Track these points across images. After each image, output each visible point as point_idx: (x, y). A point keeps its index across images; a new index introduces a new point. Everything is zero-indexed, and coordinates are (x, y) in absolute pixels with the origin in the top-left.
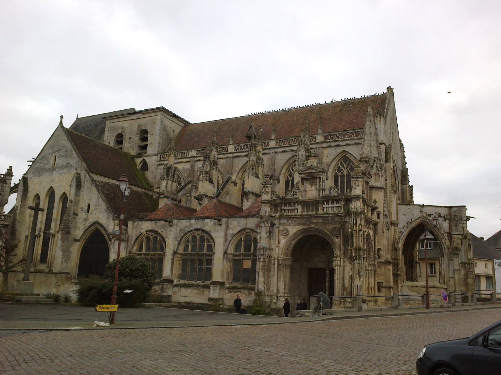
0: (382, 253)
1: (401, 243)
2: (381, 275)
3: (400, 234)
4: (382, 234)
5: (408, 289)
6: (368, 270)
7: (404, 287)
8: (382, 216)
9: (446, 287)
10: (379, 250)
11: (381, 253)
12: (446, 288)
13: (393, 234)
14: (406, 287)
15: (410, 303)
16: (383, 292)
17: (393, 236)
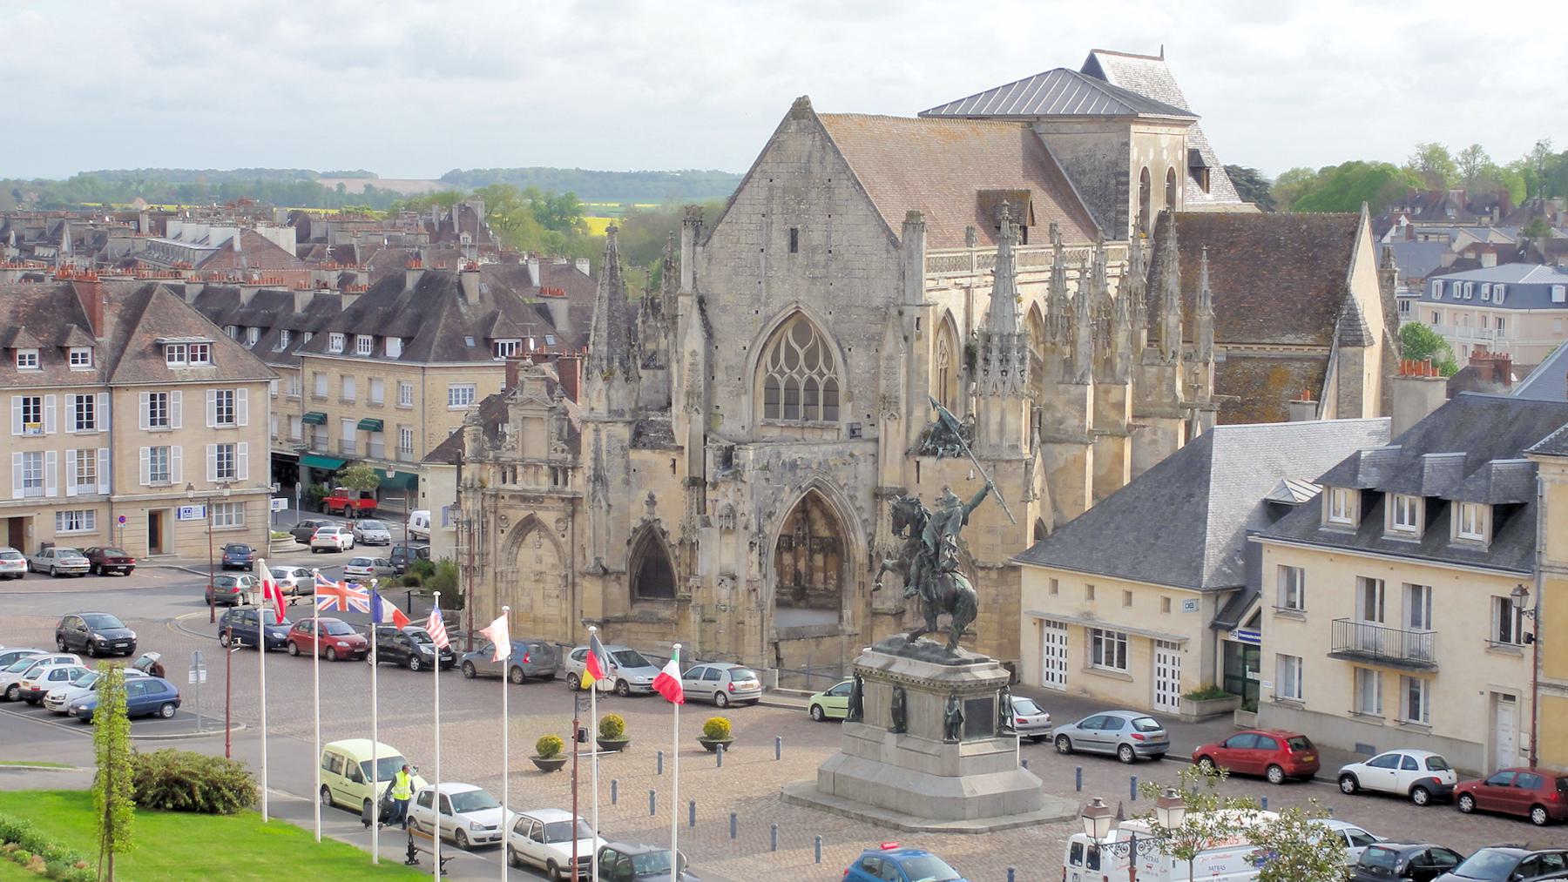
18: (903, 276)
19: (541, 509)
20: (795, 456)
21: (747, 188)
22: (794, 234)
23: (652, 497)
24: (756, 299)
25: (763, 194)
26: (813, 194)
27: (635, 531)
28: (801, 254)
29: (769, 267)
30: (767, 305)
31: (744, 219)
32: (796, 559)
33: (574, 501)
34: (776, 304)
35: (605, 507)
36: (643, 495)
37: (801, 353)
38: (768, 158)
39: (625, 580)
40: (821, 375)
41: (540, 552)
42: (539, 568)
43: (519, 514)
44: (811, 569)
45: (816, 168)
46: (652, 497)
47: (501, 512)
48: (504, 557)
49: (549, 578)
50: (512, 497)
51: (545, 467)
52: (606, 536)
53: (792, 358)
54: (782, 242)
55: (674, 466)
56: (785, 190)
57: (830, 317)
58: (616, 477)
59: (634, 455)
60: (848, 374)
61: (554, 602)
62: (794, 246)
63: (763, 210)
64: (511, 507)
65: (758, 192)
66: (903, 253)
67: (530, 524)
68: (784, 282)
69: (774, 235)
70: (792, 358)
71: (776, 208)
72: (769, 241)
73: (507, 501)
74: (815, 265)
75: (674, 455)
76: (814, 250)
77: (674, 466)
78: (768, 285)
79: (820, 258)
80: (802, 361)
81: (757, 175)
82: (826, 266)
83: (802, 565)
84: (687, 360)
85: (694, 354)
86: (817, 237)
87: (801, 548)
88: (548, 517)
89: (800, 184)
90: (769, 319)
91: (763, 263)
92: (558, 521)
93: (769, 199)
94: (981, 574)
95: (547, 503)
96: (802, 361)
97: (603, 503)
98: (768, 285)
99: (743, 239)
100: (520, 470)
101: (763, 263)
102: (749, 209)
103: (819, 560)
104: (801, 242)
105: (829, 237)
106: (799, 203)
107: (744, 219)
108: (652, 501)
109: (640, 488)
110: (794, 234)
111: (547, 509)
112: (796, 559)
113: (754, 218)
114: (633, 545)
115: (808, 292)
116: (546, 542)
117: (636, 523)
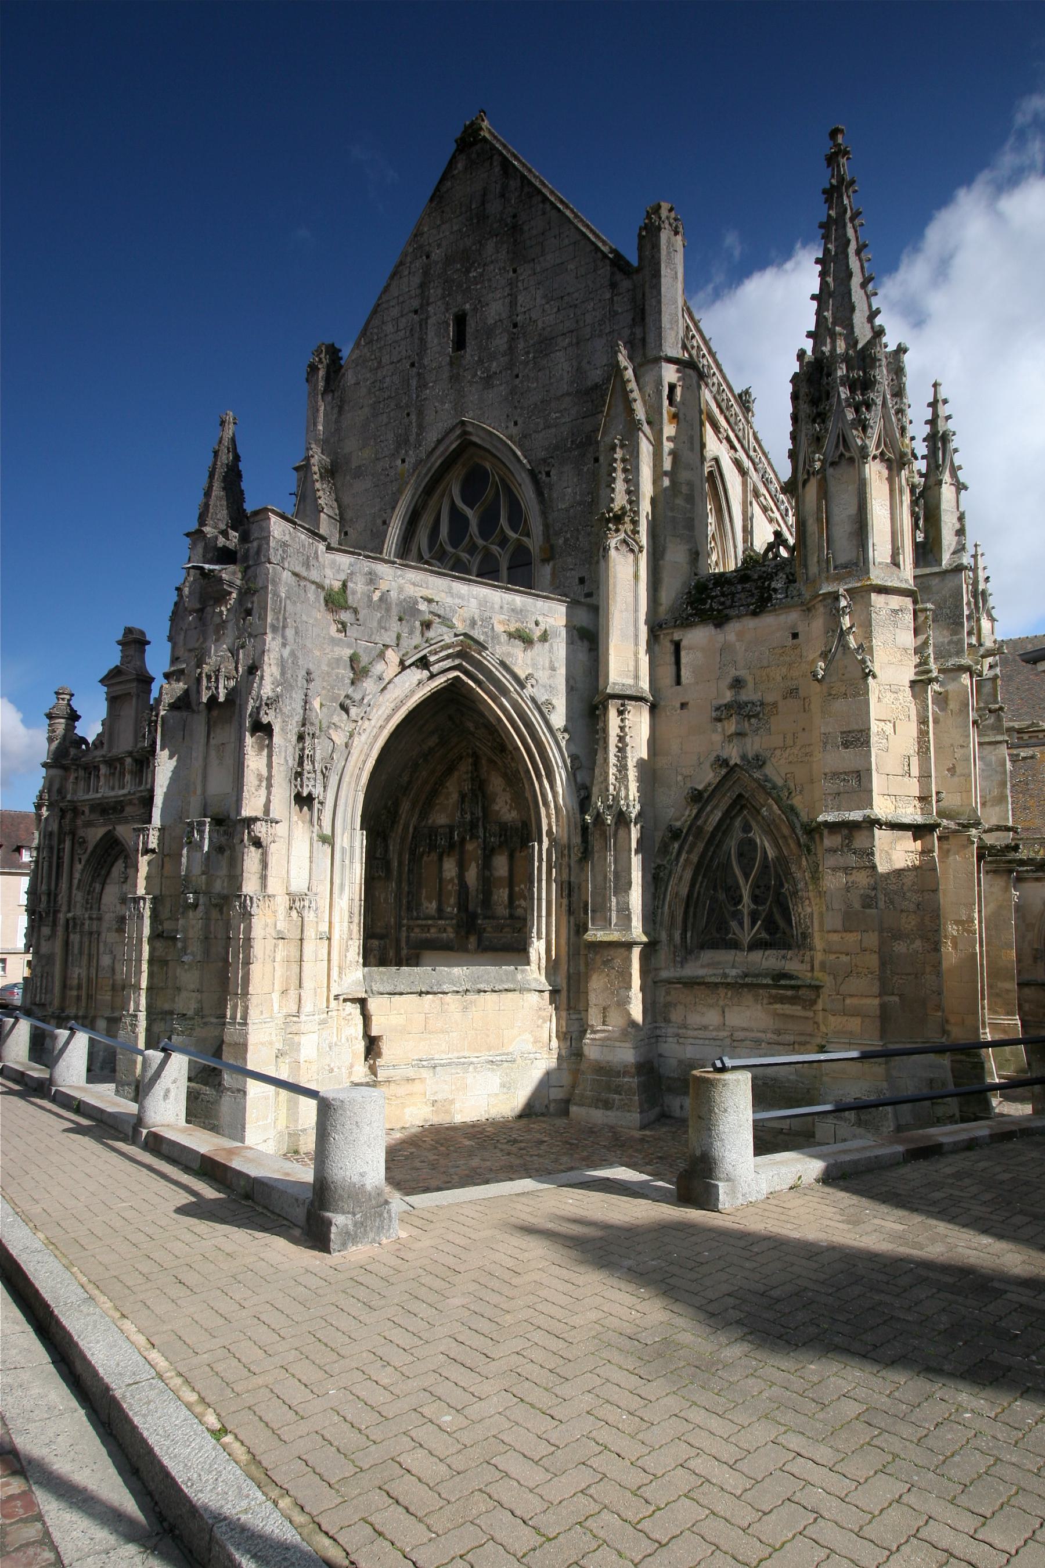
19: (120, 823)
20: (411, 591)
22: (460, 320)
25: (416, 280)
30: (418, 444)
31: (389, 328)
32: (462, 867)
37: (469, 513)
40: (503, 541)
43: (95, 834)
44: (487, 882)
48: (78, 896)
56: (448, 261)
60: (544, 514)
62: (460, 343)
63: (416, 303)
64: (89, 824)
78: (420, 413)
80: (474, 528)
83: (472, 875)
87: (470, 847)
91: (414, 383)
96: (474, 528)
99: (385, 360)
100: (103, 770)
106: (468, 271)
107: (389, 328)
110: (460, 320)
112: (462, 867)
113: (403, 321)
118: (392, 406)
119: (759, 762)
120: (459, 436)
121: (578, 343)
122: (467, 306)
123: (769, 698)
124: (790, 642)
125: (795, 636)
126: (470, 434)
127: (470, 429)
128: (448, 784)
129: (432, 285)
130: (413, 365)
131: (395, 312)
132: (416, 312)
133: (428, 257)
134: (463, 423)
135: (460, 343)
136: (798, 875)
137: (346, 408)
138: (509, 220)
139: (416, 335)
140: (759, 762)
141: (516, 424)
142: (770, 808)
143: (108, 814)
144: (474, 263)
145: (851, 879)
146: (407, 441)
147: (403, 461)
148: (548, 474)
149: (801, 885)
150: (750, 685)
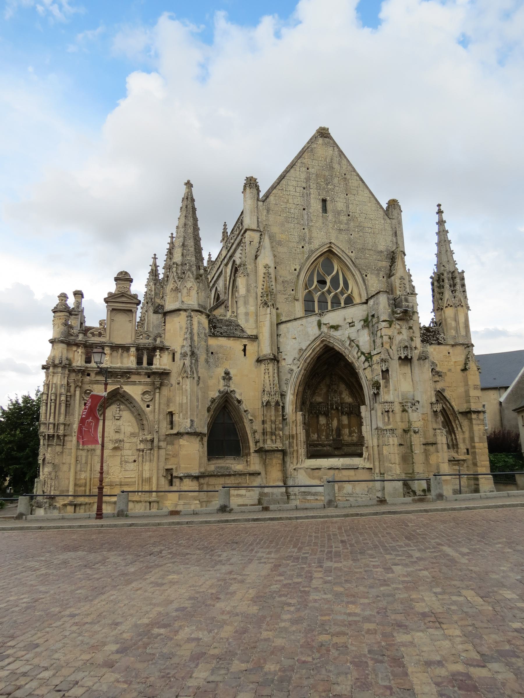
0: (177, 418)
1: (291, 389)
2: (173, 457)
3: (289, 375)
4: (177, 386)
5: (304, 473)
6: (139, 450)
7: (302, 471)
8: (178, 356)
9: (371, 466)
10: (171, 414)
11: (175, 418)
12: (371, 469)
13: (263, 378)
14: (302, 471)
15: (308, 500)
16: (175, 485)
17: (263, 382)
18: (396, 234)
19: (127, 383)
21: (292, 171)
22: (324, 201)
23: (227, 373)
24: (303, 239)
25: (303, 176)
26: (336, 180)
27: (213, 401)
28: (330, 215)
29: (309, 220)
30: (310, 243)
31: (291, 188)
33: (164, 374)
34: (316, 244)
35: (196, 379)
36: (220, 372)
38: (306, 155)
39: (205, 439)
41: (118, 423)
42: (117, 436)
45: (336, 166)
46: (227, 373)
47: (87, 387)
49: (127, 446)
50: (98, 373)
51: (133, 350)
52: (188, 402)
53: (322, 282)
54: (316, 206)
55: (244, 350)
57: (352, 254)
58: (202, 357)
59: (213, 342)
61: (132, 466)
62: (325, 210)
63: (304, 185)
65: (299, 174)
66: (394, 221)
67: (117, 397)
68: (320, 230)
69: (312, 201)
70: (322, 282)
71: (313, 186)
72: (309, 205)
73: (93, 376)
74: (340, 222)
75: (245, 341)
76: (338, 213)
77: (244, 350)
78: (310, 231)
79: (344, 218)
81: (298, 164)
82: (347, 224)
84: (261, 271)
85: (266, 267)
86: (340, 205)
88: (134, 391)
89: (327, 174)
90: (312, 252)
91: (306, 217)
92: (144, 393)
93: (308, 179)
94: (474, 416)
95: (134, 378)
97: (195, 375)
98: (310, 231)
101: (306, 217)
102: (294, 183)
103: (345, 420)
104: (330, 206)
105: (348, 207)
106: (327, 184)
108: (227, 377)
109: (217, 366)
110: (324, 201)
111: (134, 383)
113: (298, 189)
114: (212, 412)
115: (337, 238)
116: (126, 415)
117: (215, 394)
118: (296, 221)
119: (444, 390)
120: (328, 247)
121: (374, 233)
122: (328, 198)
123: (444, 371)
124: (448, 355)
125: (449, 353)
126: (332, 248)
127: (333, 246)
128: (321, 385)
129: (311, 181)
130: (304, 209)
131: (294, 183)
132: (304, 188)
133: (308, 169)
134: (330, 243)
135: (325, 210)
136: (454, 426)
137: (271, 212)
138: (343, 175)
139: (305, 198)
140: (444, 390)
141: (352, 252)
142: (446, 405)
143: (116, 377)
144: (329, 183)
145: (479, 427)
146: (304, 240)
147: (303, 247)
148: (366, 276)
149: (455, 429)
150: (438, 366)
